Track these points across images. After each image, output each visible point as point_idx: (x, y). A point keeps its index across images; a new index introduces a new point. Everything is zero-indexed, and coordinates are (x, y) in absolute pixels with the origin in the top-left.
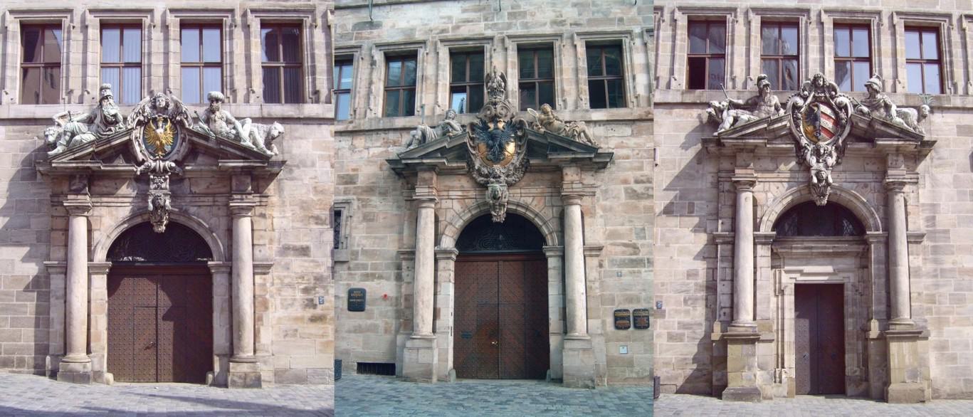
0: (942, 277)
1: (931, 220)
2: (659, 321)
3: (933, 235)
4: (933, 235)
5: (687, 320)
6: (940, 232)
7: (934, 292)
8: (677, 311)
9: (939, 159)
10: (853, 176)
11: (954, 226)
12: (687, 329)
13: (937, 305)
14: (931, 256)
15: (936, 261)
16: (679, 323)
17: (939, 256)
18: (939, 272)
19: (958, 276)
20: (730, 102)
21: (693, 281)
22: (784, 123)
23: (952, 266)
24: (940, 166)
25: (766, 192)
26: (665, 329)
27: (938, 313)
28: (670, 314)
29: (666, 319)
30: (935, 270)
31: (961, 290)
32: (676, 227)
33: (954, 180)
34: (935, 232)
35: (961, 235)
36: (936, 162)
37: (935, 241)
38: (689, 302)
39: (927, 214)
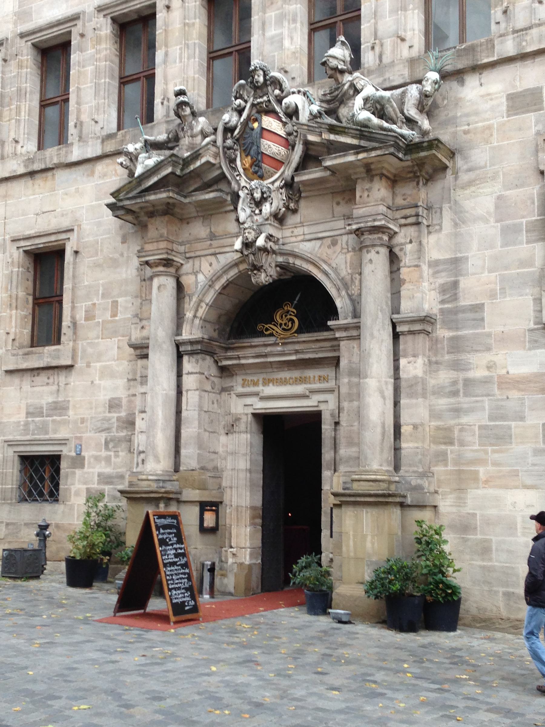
0: (466, 395)
1: (451, 290)
2: (78, 472)
3: (451, 317)
4: (451, 317)
5: (108, 470)
6: (464, 310)
7: (452, 422)
8: (97, 459)
9: (470, 170)
10: (314, 229)
11: (493, 295)
12: (107, 483)
13: (456, 447)
14: (447, 357)
15: (456, 366)
16: (99, 475)
17: (463, 356)
18: (460, 386)
19: (496, 391)
20: (146, 141)
21: (116, 415)
22: (203, 160)
23: (486, 373)
24: (470, 183)
25: (195, 273)
26: (85, 483)
27: (457, 463)
28: (89, 463)
29: (86, 470)
30: (455, 383)
31: (503, 418)
32: (98, 338)
33: (497, 207)
34: (455, 311)
35: (511, 313)
36: (464, 177)
37: (457, 329)
38: (111, 445)
39: (443, 279)
